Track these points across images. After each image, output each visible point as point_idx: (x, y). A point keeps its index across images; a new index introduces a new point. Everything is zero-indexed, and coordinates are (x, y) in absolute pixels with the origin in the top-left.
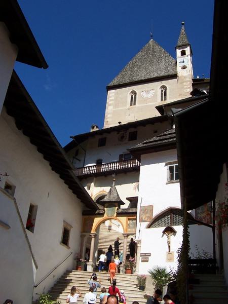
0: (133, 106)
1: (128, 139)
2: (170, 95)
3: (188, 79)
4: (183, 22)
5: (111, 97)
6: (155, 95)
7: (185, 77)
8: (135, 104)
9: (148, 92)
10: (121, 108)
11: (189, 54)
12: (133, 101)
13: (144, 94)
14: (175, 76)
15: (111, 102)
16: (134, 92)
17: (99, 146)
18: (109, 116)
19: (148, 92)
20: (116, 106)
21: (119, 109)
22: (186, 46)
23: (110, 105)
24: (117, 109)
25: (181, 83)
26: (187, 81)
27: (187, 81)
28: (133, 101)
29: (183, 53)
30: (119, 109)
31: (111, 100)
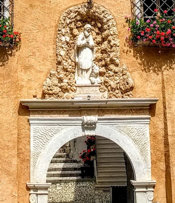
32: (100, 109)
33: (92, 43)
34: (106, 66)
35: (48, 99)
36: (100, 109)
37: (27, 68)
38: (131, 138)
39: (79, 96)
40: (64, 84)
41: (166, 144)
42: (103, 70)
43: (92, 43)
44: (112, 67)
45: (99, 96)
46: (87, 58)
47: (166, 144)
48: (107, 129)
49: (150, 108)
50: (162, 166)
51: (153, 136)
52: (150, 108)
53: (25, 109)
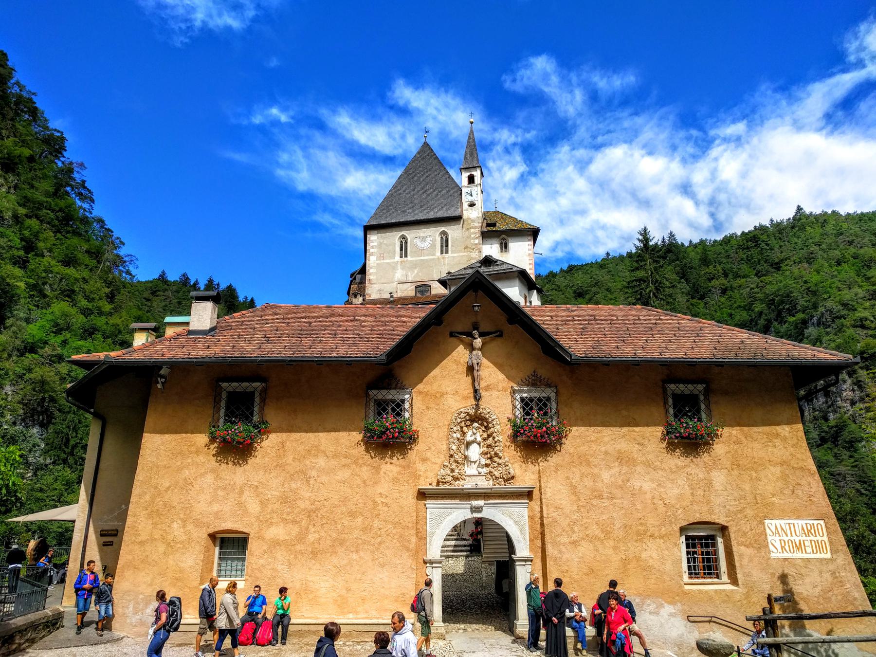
3: (476, 224)
6: (433, 245)
7: (473, 221)
8: (406, 256)
9: (423, 239)
10: (388, 261)
13: (418, 242)
14: (457, 219)
15: (372, 251)
16: (403, 237)
18: (371, 271)
19: (423, 239)
20: (381, 257)
23: (372, 254)
26: (475, 227)
27: (475, 227)
28: (404, 249)
29: (471, 180)
31: (372, 247)
32: (486, 495)
33: (479, 439)
34: (491, 458)
35: (442, 486)
36: (486, 495)
37: (424, 460)
38: (513, 520)
39: (468, 484)
40: (456, 474)
41: (542, 525)
42: (488, 462)
43: (479, 439)
44: (496, 459)
45: (485, 483)
46: (474, 452)
47: (542, 525)
48: (491, 512)
49: (528, 494)
50: (539, 543)
51: (531, 518)
52: (528, 494)
53: (422, 495)
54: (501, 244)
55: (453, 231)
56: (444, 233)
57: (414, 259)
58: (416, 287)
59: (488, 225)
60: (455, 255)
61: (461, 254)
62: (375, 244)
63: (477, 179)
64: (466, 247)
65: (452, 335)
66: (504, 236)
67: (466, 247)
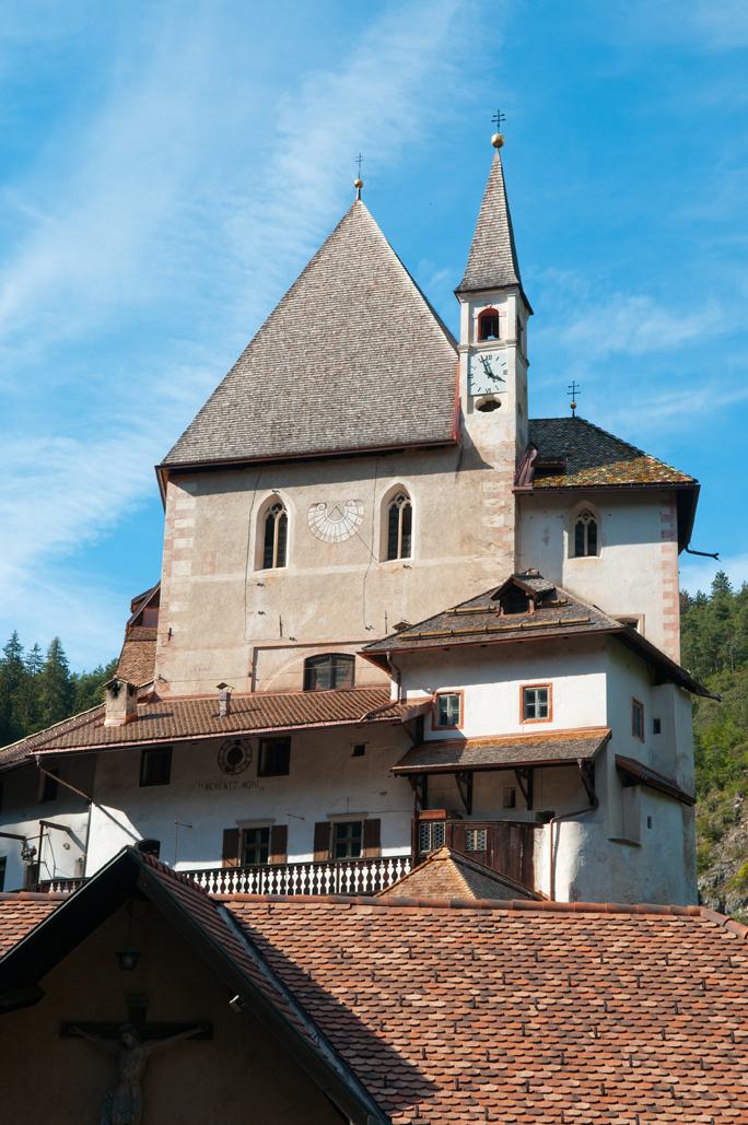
0: (275, 571)
1: (253, 768)
2: (423, 534)
4: (494, 138)
5: (182, 515)
8: (281, 563)
9: (338, 511)
11: (513, 336)
12: (272, 550)
13: (318, 517)
17: (142, 784)
18: (175, 608)
21: (219, 578)
22: (502, 289)
23: (177, 556)
24: (208, 578)
25: (474, 483)
30: (219, 578)
31: (182, 533)
54: (579, 527)
55: (425, 491)
56: (400, 495)
57: (304, 572)
58: (309, 663)
59: (540, 471)
60: (432, 562)
61: (448, 560)
62: (189, 523)
63: (507, 326)
64: (467, 539)
65: (67, 1030)
66: (585, 504)
67: (467, 539)
